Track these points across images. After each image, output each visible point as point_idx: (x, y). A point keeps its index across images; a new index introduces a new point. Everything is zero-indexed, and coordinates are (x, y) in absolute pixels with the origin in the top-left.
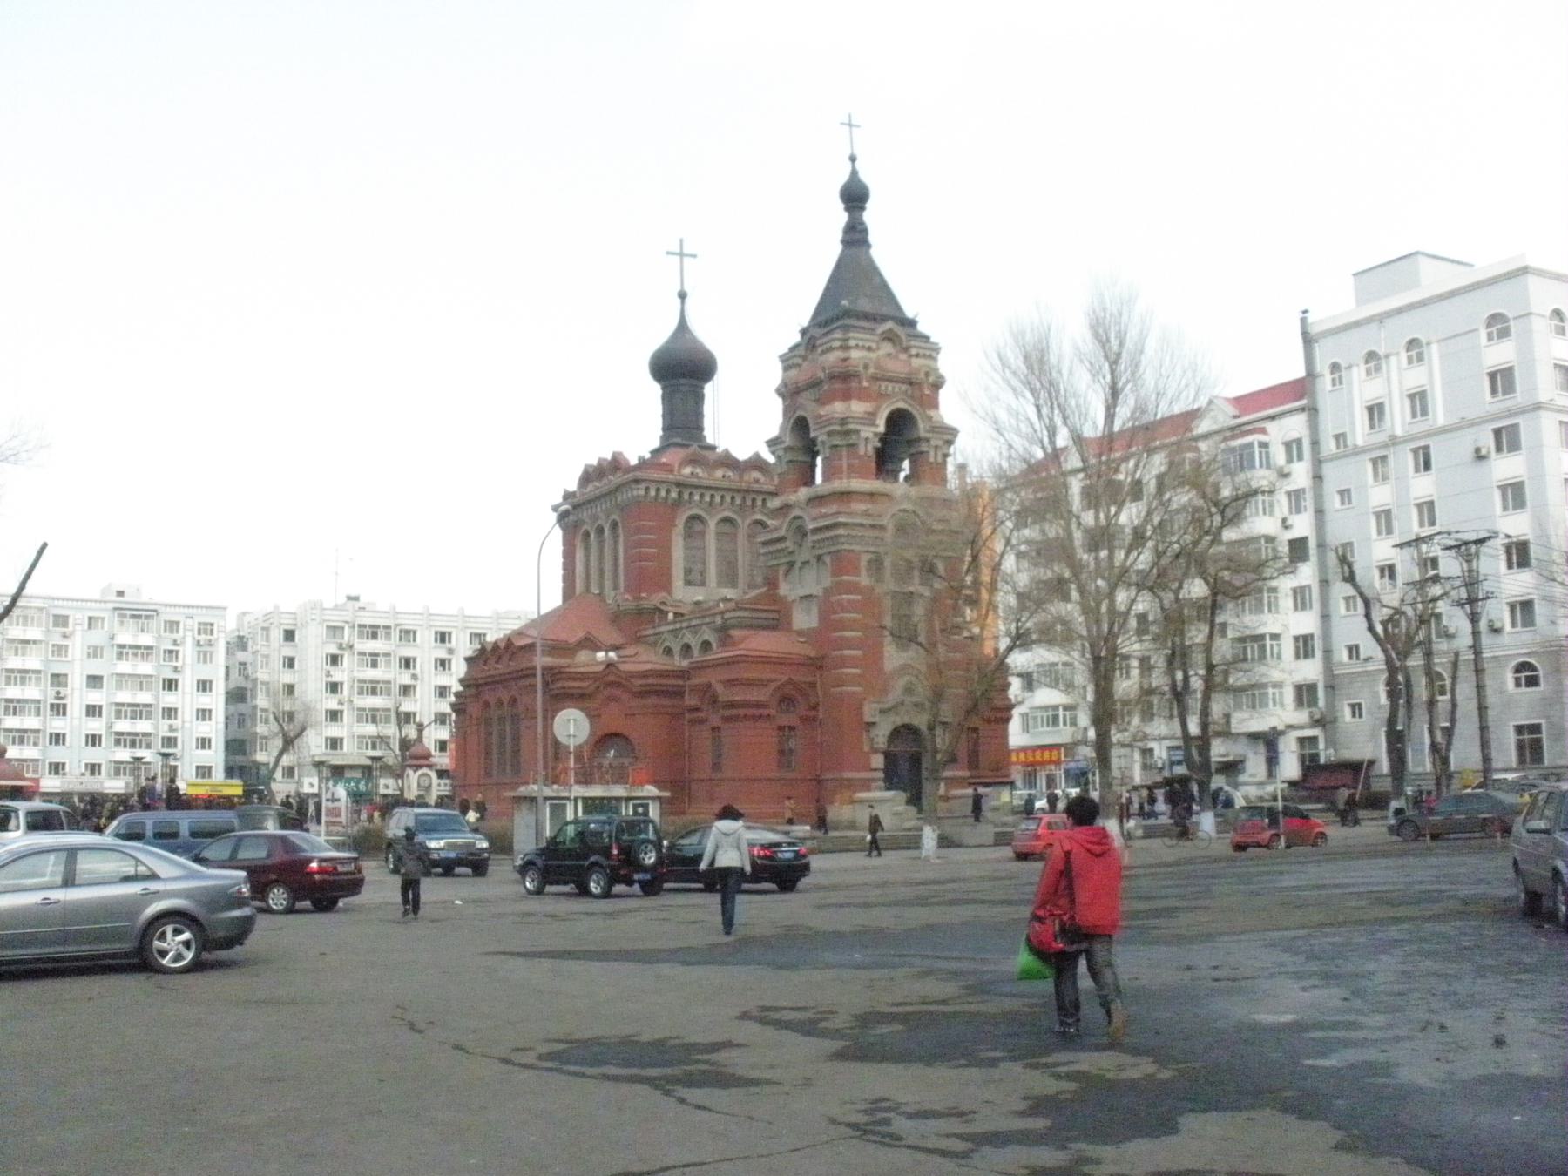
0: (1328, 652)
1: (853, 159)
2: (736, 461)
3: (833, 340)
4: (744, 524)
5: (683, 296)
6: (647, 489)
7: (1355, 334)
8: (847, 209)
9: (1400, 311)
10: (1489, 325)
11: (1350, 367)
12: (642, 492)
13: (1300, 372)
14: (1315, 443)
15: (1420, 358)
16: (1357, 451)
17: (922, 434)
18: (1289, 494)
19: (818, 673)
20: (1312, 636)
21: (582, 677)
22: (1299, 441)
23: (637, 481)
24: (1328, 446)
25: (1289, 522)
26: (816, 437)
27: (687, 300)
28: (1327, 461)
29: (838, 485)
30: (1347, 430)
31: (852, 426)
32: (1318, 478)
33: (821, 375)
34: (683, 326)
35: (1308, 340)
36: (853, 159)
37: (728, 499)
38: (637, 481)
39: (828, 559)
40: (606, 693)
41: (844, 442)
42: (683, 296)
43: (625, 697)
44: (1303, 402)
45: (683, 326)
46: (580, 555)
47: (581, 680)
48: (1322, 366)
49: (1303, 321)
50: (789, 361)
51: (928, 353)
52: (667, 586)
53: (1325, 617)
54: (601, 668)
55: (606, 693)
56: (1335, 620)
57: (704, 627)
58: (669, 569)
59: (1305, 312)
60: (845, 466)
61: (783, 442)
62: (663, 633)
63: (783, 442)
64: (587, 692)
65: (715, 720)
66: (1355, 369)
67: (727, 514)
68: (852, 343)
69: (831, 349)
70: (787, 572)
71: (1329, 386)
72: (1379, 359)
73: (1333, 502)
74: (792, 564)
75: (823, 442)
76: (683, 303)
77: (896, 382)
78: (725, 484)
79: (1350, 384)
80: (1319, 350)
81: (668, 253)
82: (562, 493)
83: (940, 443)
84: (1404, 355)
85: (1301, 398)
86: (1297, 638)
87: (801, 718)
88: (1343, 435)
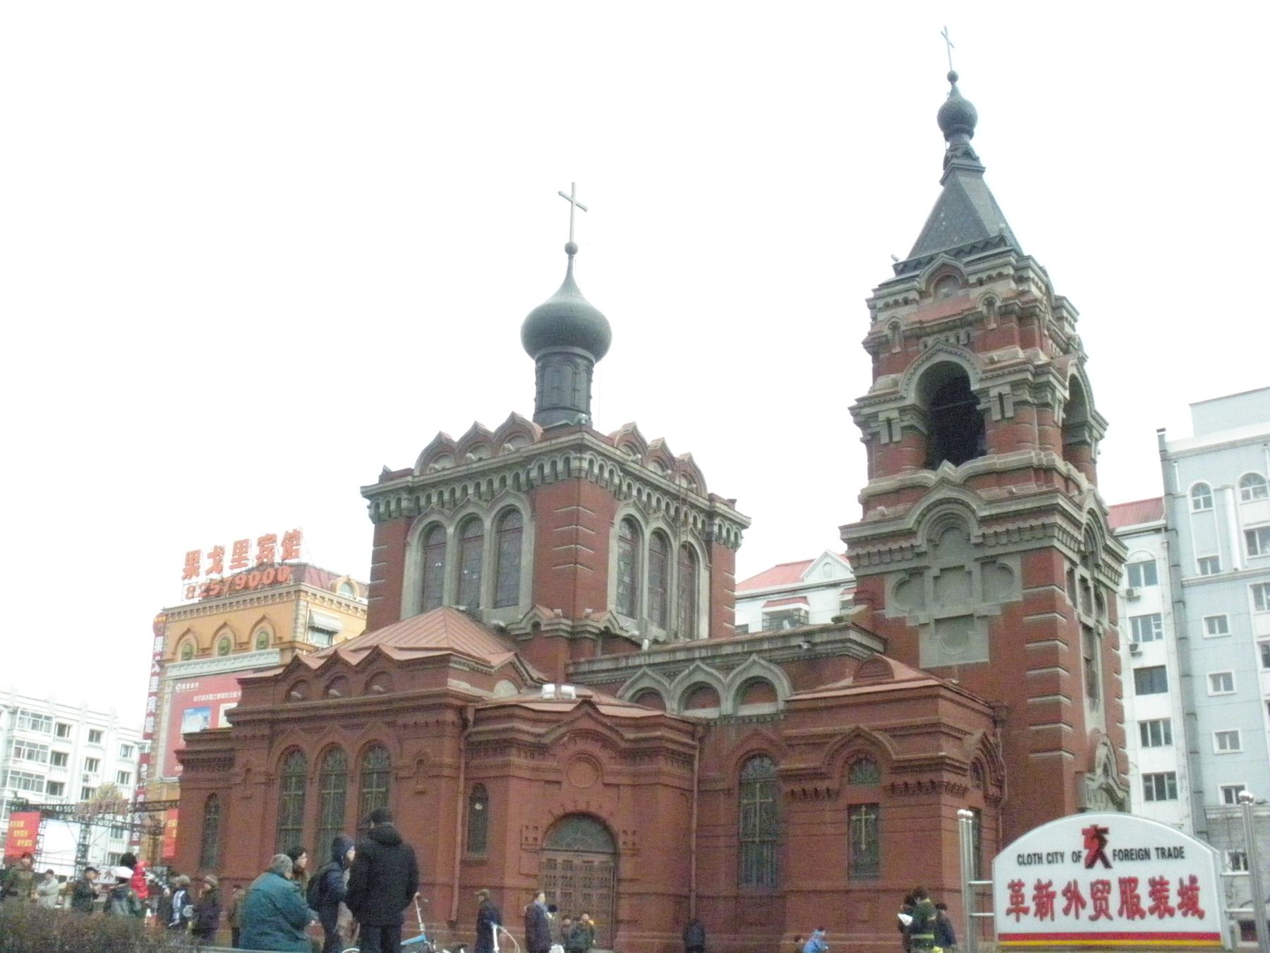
0: (1197, 793)
1: (952, 78)
2: (672, 458)
3: (1006, 265)
4: (675, 545)
5: (571, 250)
6: (591, 462)
7: (1229, 455)
8: (947, 137)
9: (1233, 445)
10: (1242, 485)
11: (1222, 489)
12: (585, 465)
13: (1160, 492)
14: (1175, 566)
15: (1208, 503)
16: (1235, 576)
17: (1090, 419)
18: (1134, 620)
19: (999, 730)
20: (1172, 776)
21: (539, 717)
22: (1150, 566)
23: (581, 448)
24: (1192, 570)
25: (1140, 649)
26: (985, 392)
27: (576, 256)
28: (1189, 586)
29: (1032, 455)
30: (1219, 554)
31: (1052, 379)
32: (1179, 603)
33: (982, 308)
34: (569, 284)
35: (1166, 459)
36: (952, 78)
37: (663, 506)
38: (581, 448)
39: (1015, 564)
40: (573, 749)
41: (1036, 401)
42: (571, 250)
43: (603, 755)
44: (1160, 522)
45: (569, 284)
46: (413, 558)
47: (535, 721)
48: (1183, 486)
49: (1161, 438)
50: (882, 300)
51: (1073, 322)
52: (601, 607)
53: (1193, 753)
54: (569, 707)
55: (573, 749)
56: (1206, 757)
57: (754, 657)
58: (605, 584)
59: (1163, 430)
60: (1037, 432)
61: (902, 398)
62: (640, 666)
63: (902, 398)
64: (546, 741)
65: (859, 792)
66: (1229, 492)
67: (661, 524)
68: (1032, 275)
69: (1000, 276)
70: (901, 584)
71: (1191, 509)
72: (1208, 492)
73: (1198, 630)
74: (916, 573)
75: (1001, 396)
76: (571, 258)
77: (1057, 345)
78: (664, 483)
79: (1223, 506)
80: (1178, 470)
81: (560, 194)
82: (380, 472)
83: (1098, 437)
84: (1239, 491)
85: (1158, 518)
86: (1147, 778)
87: (986, 797)
88: (1214, 560)
